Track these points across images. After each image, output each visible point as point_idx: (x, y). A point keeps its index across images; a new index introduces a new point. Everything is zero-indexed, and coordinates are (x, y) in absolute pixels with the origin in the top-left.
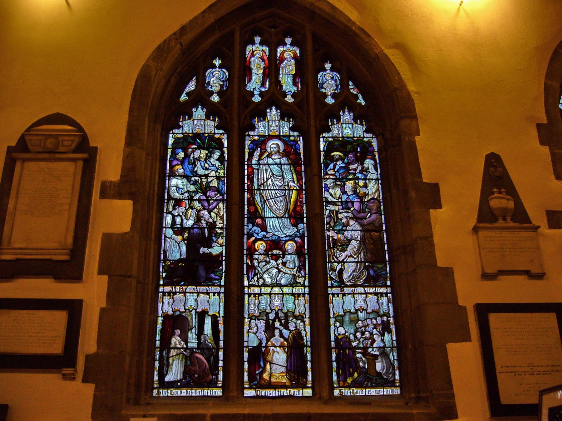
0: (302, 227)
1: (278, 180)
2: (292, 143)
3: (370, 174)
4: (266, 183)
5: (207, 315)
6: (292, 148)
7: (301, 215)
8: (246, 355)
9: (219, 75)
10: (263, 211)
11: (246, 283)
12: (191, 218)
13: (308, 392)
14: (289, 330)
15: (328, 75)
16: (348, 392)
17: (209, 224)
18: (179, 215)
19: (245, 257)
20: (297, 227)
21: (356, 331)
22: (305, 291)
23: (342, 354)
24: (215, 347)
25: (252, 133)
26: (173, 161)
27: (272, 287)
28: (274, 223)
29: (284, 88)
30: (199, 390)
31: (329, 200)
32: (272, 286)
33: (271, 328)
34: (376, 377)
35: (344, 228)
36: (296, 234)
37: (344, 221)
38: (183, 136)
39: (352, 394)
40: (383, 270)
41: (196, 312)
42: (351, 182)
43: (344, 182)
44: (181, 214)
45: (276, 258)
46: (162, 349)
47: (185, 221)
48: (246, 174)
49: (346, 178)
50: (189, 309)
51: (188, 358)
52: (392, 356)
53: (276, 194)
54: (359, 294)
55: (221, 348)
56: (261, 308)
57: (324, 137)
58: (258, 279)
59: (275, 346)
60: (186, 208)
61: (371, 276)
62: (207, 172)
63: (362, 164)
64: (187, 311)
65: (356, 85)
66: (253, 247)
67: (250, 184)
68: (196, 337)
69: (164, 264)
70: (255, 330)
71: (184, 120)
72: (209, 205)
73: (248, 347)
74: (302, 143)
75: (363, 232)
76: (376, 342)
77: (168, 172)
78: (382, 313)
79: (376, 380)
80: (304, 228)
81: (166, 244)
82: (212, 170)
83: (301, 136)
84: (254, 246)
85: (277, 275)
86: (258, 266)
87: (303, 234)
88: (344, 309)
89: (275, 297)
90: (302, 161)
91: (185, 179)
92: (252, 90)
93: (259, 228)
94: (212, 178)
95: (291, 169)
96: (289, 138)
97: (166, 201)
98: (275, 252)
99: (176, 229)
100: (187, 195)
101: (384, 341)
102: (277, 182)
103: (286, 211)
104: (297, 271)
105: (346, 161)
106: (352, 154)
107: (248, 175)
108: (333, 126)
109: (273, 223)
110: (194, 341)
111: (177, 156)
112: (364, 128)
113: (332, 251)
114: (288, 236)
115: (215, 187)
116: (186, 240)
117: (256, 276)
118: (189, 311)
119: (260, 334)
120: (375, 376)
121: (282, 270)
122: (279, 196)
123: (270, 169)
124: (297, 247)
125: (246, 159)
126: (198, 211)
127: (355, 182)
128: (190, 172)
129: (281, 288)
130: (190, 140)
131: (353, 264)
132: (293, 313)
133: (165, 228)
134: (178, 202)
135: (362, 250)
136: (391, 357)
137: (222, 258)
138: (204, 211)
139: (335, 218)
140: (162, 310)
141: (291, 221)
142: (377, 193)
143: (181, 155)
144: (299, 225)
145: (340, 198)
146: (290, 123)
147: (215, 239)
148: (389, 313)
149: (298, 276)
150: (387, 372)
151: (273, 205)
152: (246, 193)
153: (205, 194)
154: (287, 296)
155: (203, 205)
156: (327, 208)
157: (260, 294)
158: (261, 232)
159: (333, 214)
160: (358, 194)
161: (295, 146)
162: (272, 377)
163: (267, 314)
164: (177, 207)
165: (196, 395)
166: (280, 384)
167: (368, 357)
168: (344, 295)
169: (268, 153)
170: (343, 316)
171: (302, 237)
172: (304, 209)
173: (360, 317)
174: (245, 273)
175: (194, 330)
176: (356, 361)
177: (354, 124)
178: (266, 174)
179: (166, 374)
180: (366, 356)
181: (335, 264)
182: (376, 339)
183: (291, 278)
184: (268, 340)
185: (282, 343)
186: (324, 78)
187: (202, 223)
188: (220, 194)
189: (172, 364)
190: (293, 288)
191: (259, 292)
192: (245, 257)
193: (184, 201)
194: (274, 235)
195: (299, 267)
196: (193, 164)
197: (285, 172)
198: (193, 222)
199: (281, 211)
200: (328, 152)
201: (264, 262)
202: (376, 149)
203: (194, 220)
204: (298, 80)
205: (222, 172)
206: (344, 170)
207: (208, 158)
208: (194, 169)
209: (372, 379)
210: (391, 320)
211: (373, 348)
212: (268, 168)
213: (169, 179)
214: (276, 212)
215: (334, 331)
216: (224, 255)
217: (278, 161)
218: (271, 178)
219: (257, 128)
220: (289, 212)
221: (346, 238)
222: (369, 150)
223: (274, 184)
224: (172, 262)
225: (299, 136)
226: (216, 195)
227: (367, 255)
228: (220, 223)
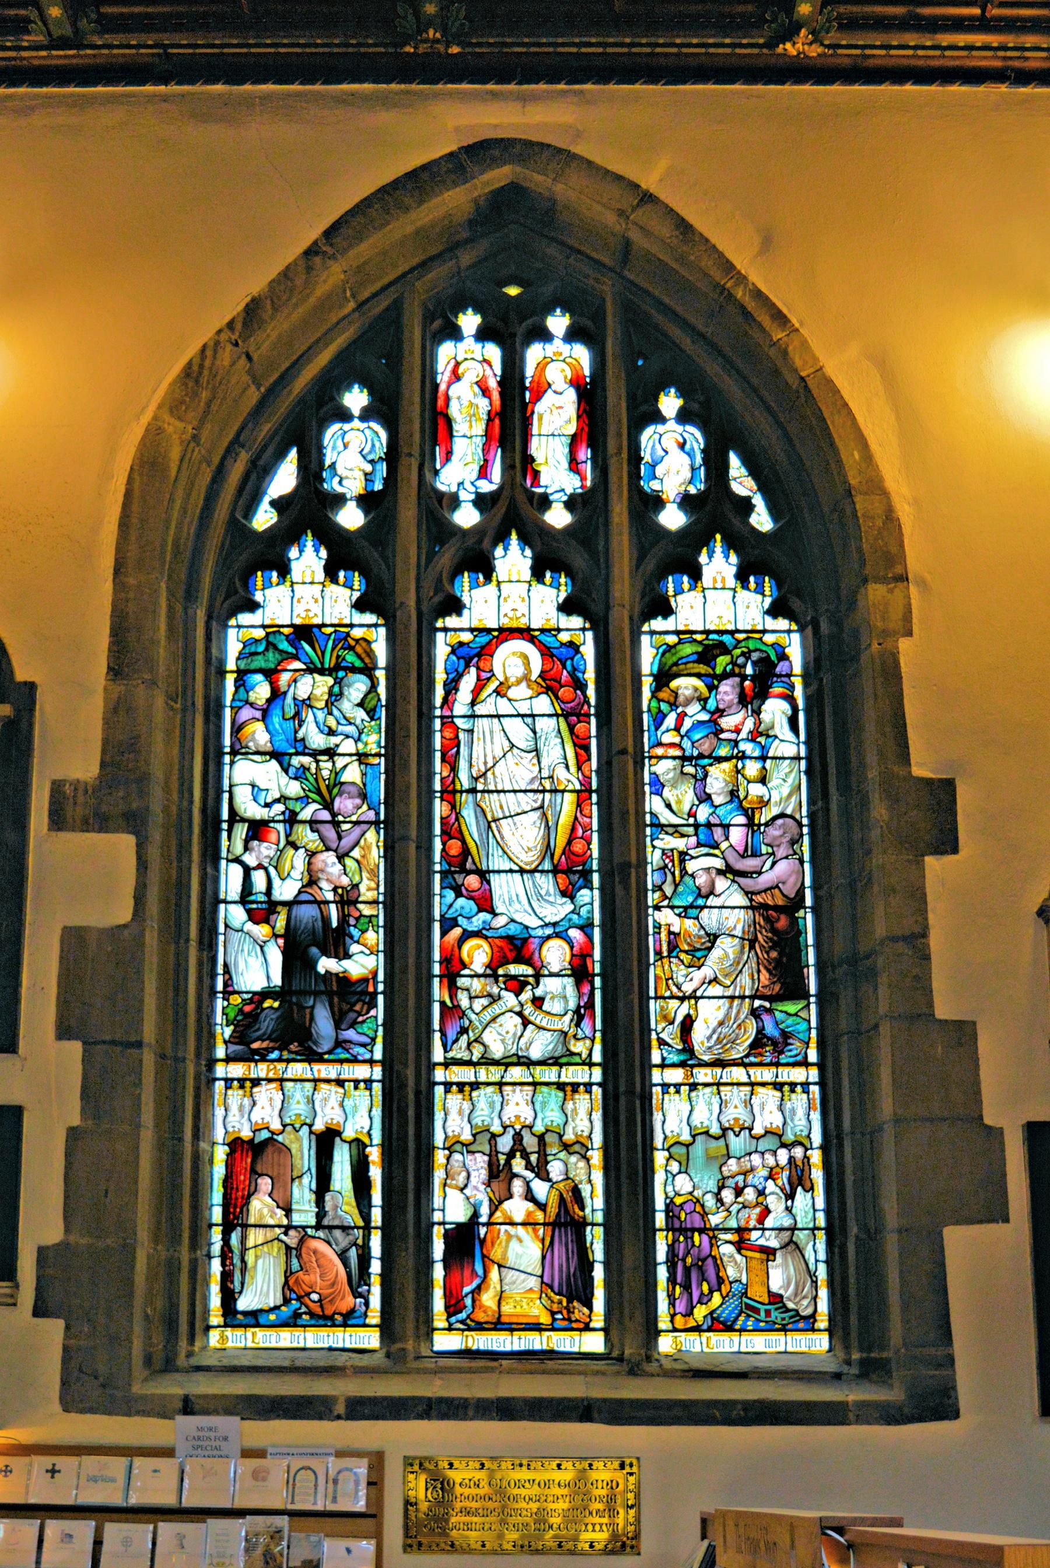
0: (587, 900)
3: (777, 741)
5: (337, 1140)
6: (564, 667)
7: (584, 864)
8: (438, 1248)
10: (483, 853)
11: (438, 1055)
13: (594, 1343)
14: (550, 1180)
16: (694, 1344)
17: (340, 891)
18: (260, 866)
19: (436, 981)
20: (572, 898)
21: (721, 1188)
23: (682, 1246)
24: (361, 1223)
26: (240, 708)
27: (507, 1065)
29: (543, 481)
31: (663, 821)
32: (504, 1063)
34: (770, 1303)
35: (700, 902)
37: (702, 880)
39: (706, 1350)
40: (799, 1020)
41: (311, 1132)
42: (726, 766)
43: (704, 767)
45: (517, 985)
47: (276, 881)
48: (438, 745)
49: (710, 757)
51: (294, 1252)
53: (519, 803)
54: (732, 1084)
55: (376, 1228)
56: (477, 1121)
58: (469, 1044)
59: (512, 1224)
61: (765, 1036)
62: (334, 740)
63: (757, 712)
64: (289, 1128)
65: (754, 470)
68: (313, 1197)
70: (461, 1179)
71: (267, 585)
72: (340, 838)
73: (443, 1223)
75: (750, 912)
76: (771, 1216)
78: (789, 1137)
79: (768, 1313)
81: (229, 946)
82: (347, 737)
86: (471, 1008)
88: (693, 1124)
90: (589, 706)
91: (273, 761)
92: (454, 489)
93: (472, 902)
94: (347, 759)
95: (559, 731)
97: (225, 826)
98: (515, 969)
100: (279, 808)
105: (711, 704)
110: (307, 1207)
112: (768, 601)
113: (666, 967)
115: (353, 783)
117: (465, 1036)
121: (532, 1019)
124: (573, 955)
125: (438, 701)
126: (312, 854)
130: (284, 646)
131: (722, 1001)
132: (561, 1136)
133: (225, 902)
134: (258, 830)
136: (809, 1253)
137: (376, 988)
138: (326, 854)
139: (677, 873)
142: (793, 799)
143: (261, 691)
145: (692, 814)
149: (575, 1036)
150: (796, 1295)
152: (437, 802)
153: (328, 806)
154: (545, 1089)
155: (322, 839)
156: (655, 843)
157: (475, 1085)
159: (673, 861)
160: (741, 802)
161: (572, 659)
162: (503, 1303)
163: (494, 1136)
164: (256, 843)
166: (524, 1320)
167: (749, 1254)
168: (693, 1087)
169: (497, 683)
170: (687, 1146)
171: (586, 927)
173: (732, 1147)
175: (306, 1180)
176: (718, 1264)
177: (739, 589)
179: (241, 1293)
180: (743, 1252)
181: (674, 1004)
182: (771, 1207)
184: (494, 1206)
185: (529, 1214)
186: (658, 446)
189: (255, 1267)
191: (473, 1079)
192: (436, 981)
194: (513, 921)
195: (577, 1011)
196: (293, 718)
198: (299, 885)
200: (663, 677)
202: (797, 669)
204: (585, 454)
205: (374, 741)
207: (334, 697)
208: (296, 732)
209: (757, 1311)
210: (816, 1157)
213: (232, 763)
216: (381, 977)
217: (524, 708)
220: (552, 856)
225: (584, 629)
228: (369, 889)
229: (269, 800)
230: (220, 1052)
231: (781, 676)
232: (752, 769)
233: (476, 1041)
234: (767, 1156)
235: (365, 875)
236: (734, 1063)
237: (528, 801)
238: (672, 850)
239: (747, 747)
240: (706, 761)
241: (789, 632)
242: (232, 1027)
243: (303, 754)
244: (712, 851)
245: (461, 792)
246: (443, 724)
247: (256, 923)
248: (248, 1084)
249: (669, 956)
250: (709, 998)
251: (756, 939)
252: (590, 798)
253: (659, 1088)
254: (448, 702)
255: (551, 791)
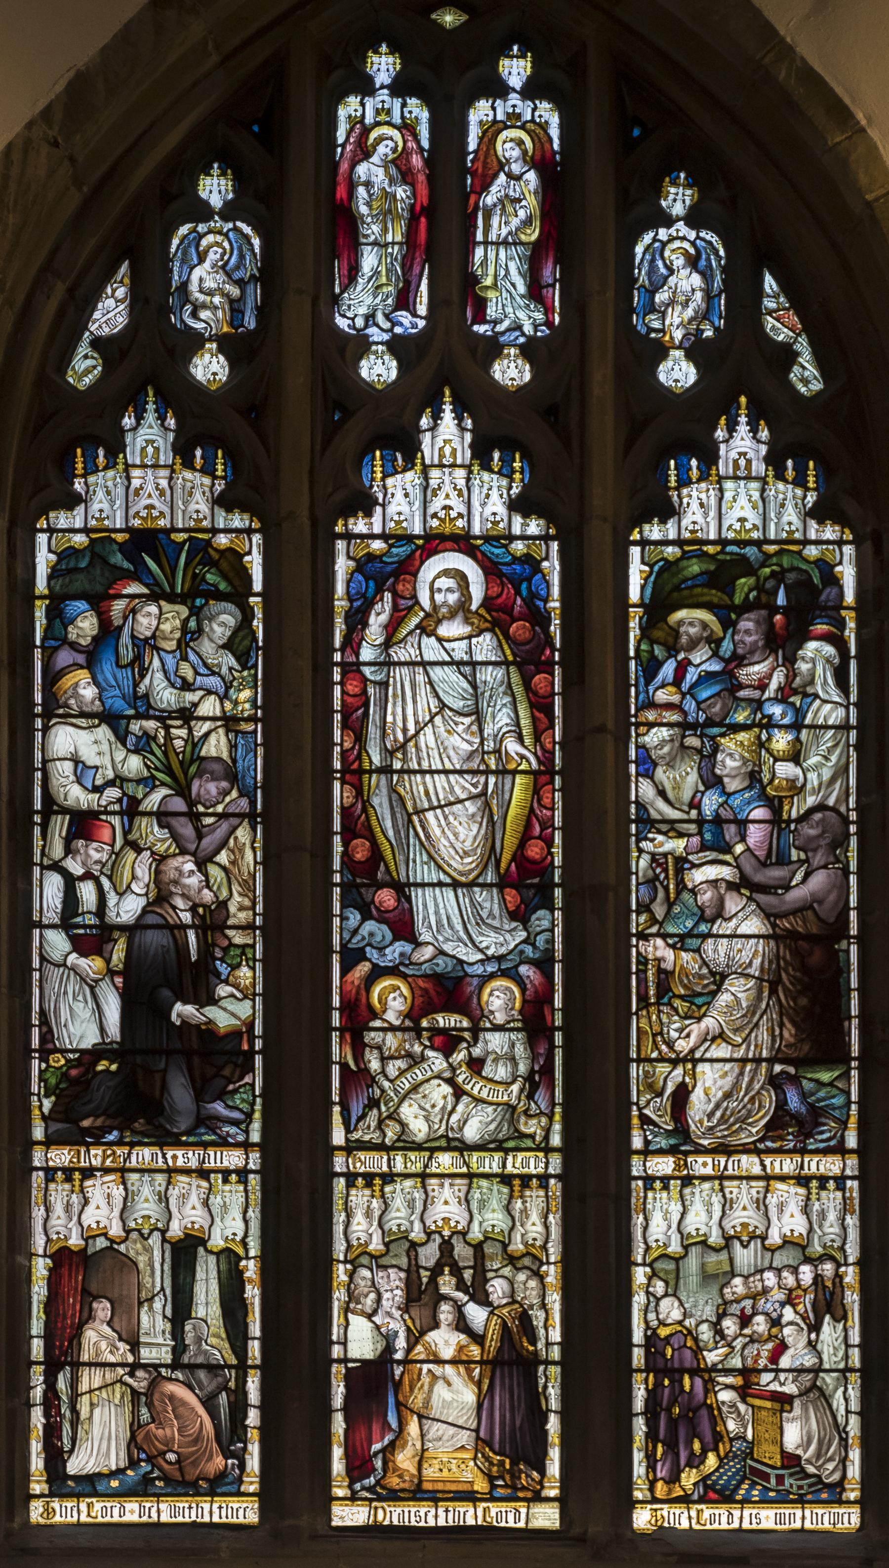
0: (546, 924)
1: (460, 728)
2: (517, 567)
3: (818, 702)
4: (412, 744)
6: (518, 592)
9: (224, 253)
10: (400, 858)
11: (338, 1137)
12: (134, 886)
14: (488, 1304)
15: (677, 244)
18: (88, 876)
19: (335, 1036)
22: (547, 1167)
23: (667, 1391)
25: (359, 526)
26: (56, 649)
27: (433, 1150)
28: (441, 905)
30: (181, 1505)
31: (654, 815)
32: (430, 1147)
33: (425, 1298)
34: (783, 1467)
35: (703, 928)
36: (522, 952)
37: (706, 897)
38: (91, 540)
42: (742, 736)
43: (713, 738)
44: (96, 870)
46: (52, 1368)
47: (112, 899)
48: (337, 705)
50: (139, 1231)
51: (143, 1399)
52: (842, 1401)
53: (452, 788)
57: (644, 543)
60: (112, 846)
61: (788, 1113)
63: (790, 661)
66: (364, 1000)
67: (353, 748)
69: (44, 1065)
70: (369, 1301)
71: (91, 469)
72: (200, 836)
74: (558, 567)
75: (772, 943)
76: (790, 1352)
77: (38, 698)
80: (553, 926)
81: (47, 987)
82: (209, 692)
83: (553, 538)
84: (368, 998)
85: (449, 1108)
86: (383, 1072)
87: (549, 953)
88: (685, 1232)
89: (442, 1185)
90: (553, 649)
93: (385, 927)
94: (207, 726)
95: (509, 686)
96: (505, 546)
97: (37, 819)
98: (443, 1020)
99: (81, 931)
100: (113, 793)
101: (819, 1347)
102: (455, 740)
103: (489, 857)
104: (522, 1090)
105: (727, 647)
106: (752, 615)
107: (346, 713)
108: (685, 491)
109: (436, 905)
111: (70, 629)
112: (811, 498)
114: (493, 957)
115: (218, 759)
116: (117, 973)
117: (375, 1111)
118: (142, 1235)
119: (387, 1320)
120: (779, 1464)
122: (463, 796)
123: (431, 683)
124: (524, 1001)
126: (161, 859)
127: (759, 737)
128: (124, 698)
129: (462, 1155)
130: (118, 559)
131: (728, 1066)
133: (42, 926)
135: (765, 1011)
137: (252, 1044)
138: (180, 859)
140: (46, 1234)
141: (504, 900)
144: (534, 917)
145: (695, 804)
146: (512, 480)
147: (223, 969)
148: (842, 1249)
149: (526, 1112)
151: (438, 832)
152: (337, 785)
153: (182, 790)
156: (644, 845)
158: (391, 944)
159: (666, 870)
161: (529, 580)
164: (81, 843)
165: (174, 1520)
167: (757, 1402)
169: (422, 614)
171: (544, 964)
172: (557, 851)
173: (738, 1261)
174: (336, 1098)
176: (715, 1415)
178: (415, 702)
181: (662, 1069)
182: (789, 1341)
183: (499, 1119)
187: (174, 908)
188: (239, 790)
190: (506, 1154)
191: (385, 1168)
193: (103, 817)
194: (442, 953)
195: (529, 1078)
196: (131, 664)
197: (487, 694)
198: (142, 902)
199: (470, 860)
201: (403, 1057)
202: (850, 597)
203: (146, 894)
206: (716, 689)
208: (136, 685)
210: (851, 1275)
211: (777, 1371)
212: (420, 678)
213: (46, 729)
214: (452, 862)
215: (646, 1311)
216: (258, 1030)
217: (459, 650)
218: (431, 720)
219: (381, 501)
220: (498, 862)
221: (708, 966)
222: (823, 597)
223: (445, 749)
224: (71, 1056)
226: (227, 793)
227: (781, 1034)
228: (241, 908)
229: (99, 782)
230: (38, 1133)
231: (826, 608)
232: (781, 741)
233: (389, 1117)
234: (785, 1274)
235: (236, 888)
236: (746, 1150)
237: (462, 786)
238: (665, 855)
239: (776, 710)
240: (715, 731)
241: (840, 543)
242: (53, 1098)
243: (148, 717)
244: (722, 857)
245: (370, 772)
246: (343, 674)
247: (84, 954)
248: (77, 1175)
249: (658, 1003)
250: (712, 1061)
251: (779, 980)
252: (552, 782)
253: (640, 1183)
254: (352, 643)
255: (496, 772)
